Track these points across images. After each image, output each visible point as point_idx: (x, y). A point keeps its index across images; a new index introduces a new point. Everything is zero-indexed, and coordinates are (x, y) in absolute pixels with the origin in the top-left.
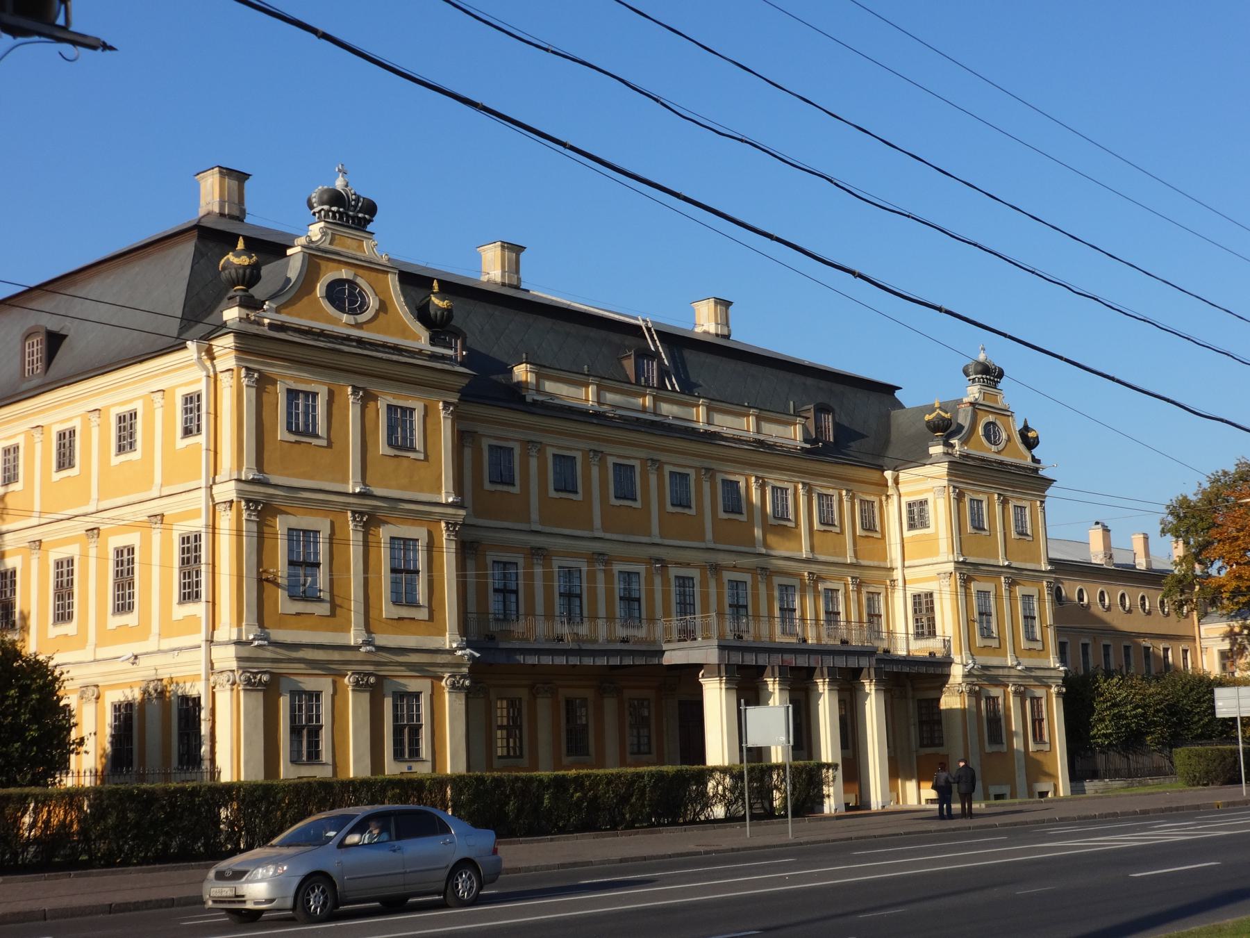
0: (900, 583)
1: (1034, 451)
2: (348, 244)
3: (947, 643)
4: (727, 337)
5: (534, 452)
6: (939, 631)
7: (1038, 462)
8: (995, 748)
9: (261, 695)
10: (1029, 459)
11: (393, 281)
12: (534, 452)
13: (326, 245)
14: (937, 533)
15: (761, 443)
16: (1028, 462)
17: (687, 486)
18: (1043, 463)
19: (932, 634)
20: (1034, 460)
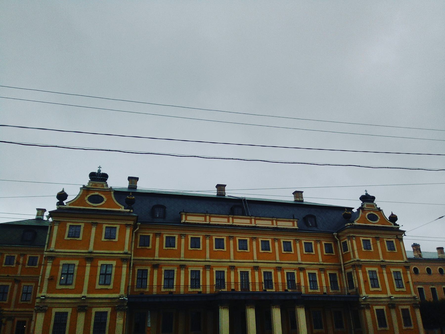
0: (343, 270)
1: (396, 222)
2: (99, 185)
3: (356, 289)
4: (302, 201)
5: (183, 237)
6: (355, 286)
7: (398, 225)
8: (383, 329)
9: (44, 314)
10: (393, 224)
11: (112, 193)
12: (183, 237)
13: (90, 187)
14: (350, 252)
15: (277, 228)
16: (393, 226)
17: (247, 243)
18: (400, 225)
19: (354, 288)
20: (396, 225)
